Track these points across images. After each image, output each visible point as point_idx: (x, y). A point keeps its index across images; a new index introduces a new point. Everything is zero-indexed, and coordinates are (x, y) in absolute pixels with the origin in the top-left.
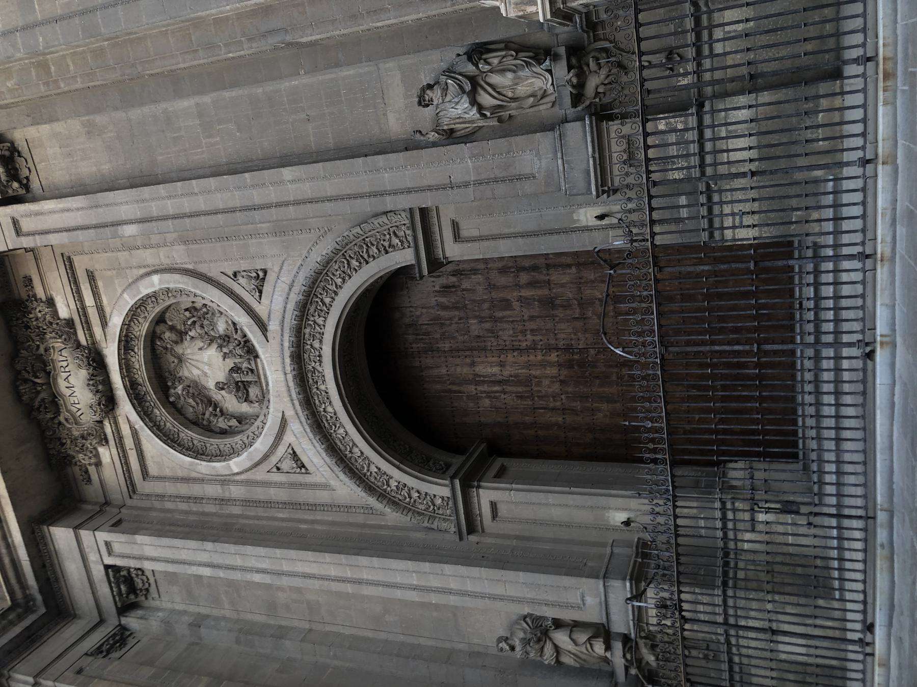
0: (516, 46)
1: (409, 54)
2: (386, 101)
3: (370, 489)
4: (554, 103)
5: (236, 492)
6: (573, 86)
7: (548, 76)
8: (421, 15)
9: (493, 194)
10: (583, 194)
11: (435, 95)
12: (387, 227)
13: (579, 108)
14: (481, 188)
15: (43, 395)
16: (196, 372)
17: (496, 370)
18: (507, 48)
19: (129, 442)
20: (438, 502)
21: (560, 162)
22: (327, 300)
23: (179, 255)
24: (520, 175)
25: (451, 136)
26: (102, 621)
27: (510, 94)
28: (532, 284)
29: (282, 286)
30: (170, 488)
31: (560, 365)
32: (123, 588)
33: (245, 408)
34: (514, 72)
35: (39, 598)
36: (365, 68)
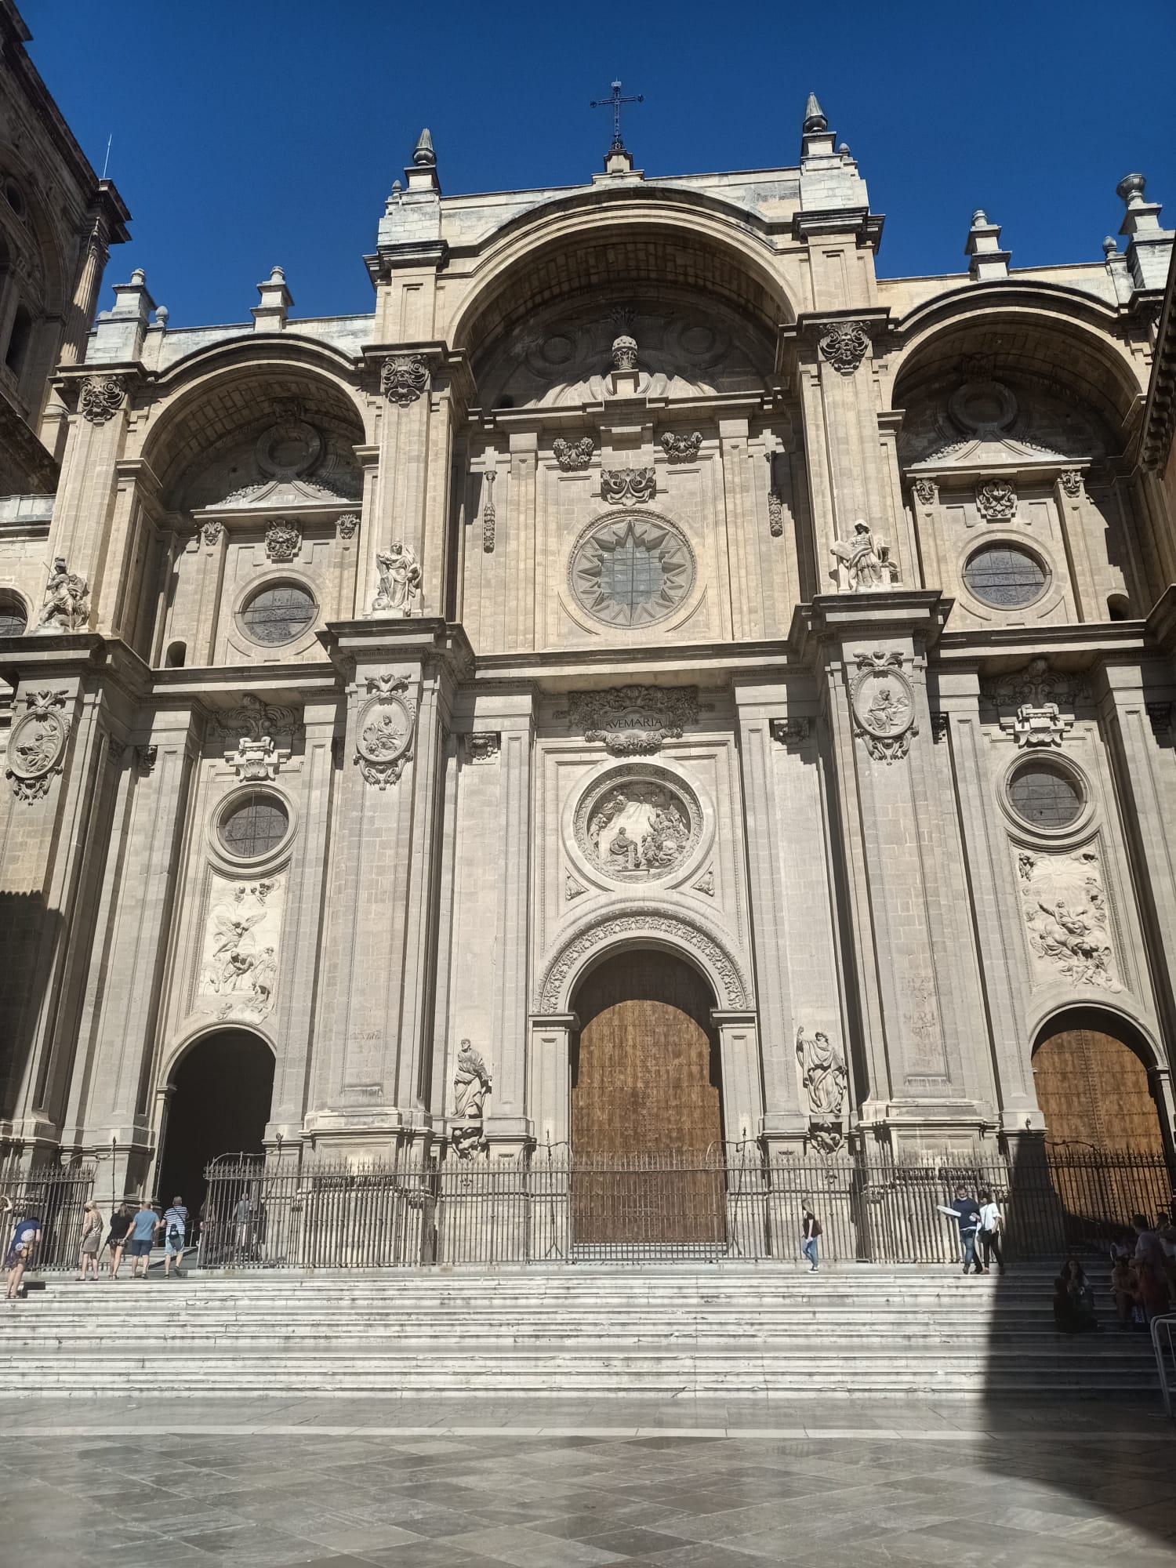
3: (562, 951)
5: (551, 840)
15: (628, 703)
16: (632, 810)
17: (630, 1042)
19: (586, 757)
20: (553, 1000)
22: (694, 940)
23: (726, 833)
25: (800, 1048)
26: (452, 717)
28: (691, 1074)
29: (703, 908)
30: (550, 784)
31: (634, 1088)
32: (481, 741)
33: (604, 846)
35: (479, 675)
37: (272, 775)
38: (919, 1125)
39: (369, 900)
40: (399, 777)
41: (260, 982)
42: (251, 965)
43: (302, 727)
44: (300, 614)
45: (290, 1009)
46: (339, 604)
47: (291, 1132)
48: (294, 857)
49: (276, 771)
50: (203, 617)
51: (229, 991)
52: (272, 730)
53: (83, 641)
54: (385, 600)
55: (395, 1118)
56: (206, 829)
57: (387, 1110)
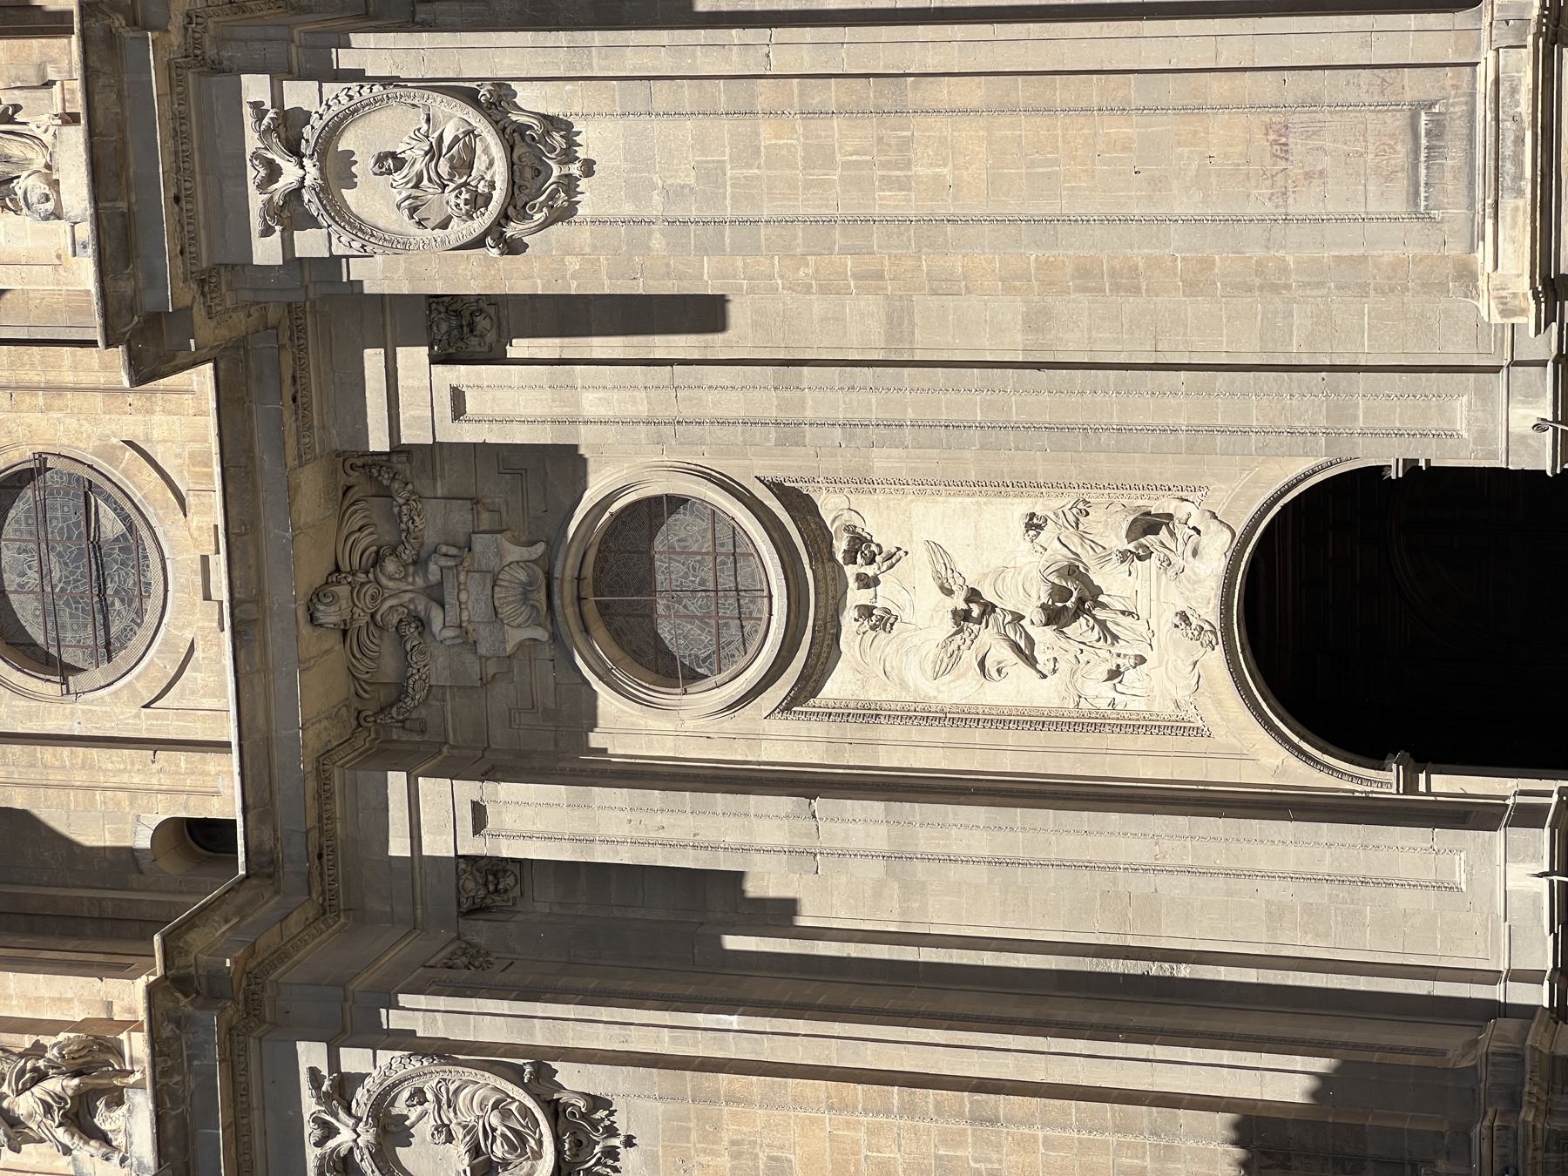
37: (540, 548)
39: (903, 185)
40: (551, 122)
41: (1118, 540)
42: (1072, 571)
43: (399, 449)
44: (64, 512)
45: (1193, 431)
46: (32, 389)
47: (1531, 396)
48: (769, 475)
49: (531, 543)
50: (80, 778)
51: (1141, 626)
52: (408, 555)
53: (167, 1030)
54: (29, 184)
55: (1510, 58)
56: (690, 725)
57: (1483, 85)
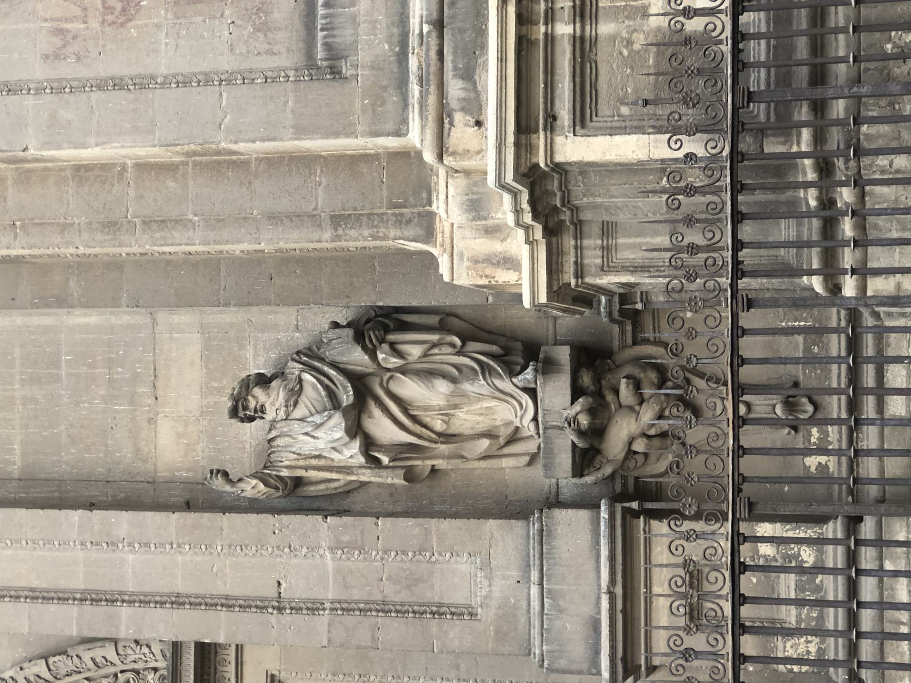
0: (464, 325)
1: (227, 305)
2: (160, 393)
4: (533, 458)
6: (580, 433)
7: (526, 399)
8: (262, 246)
9: (374, 639)
10: (580, 672)
11: (272, 400)
12: (112, 670)
13: (588, 479)
14: (349, 620)
18: (442, 328)
21: (534, 590)
24: (441, 605)
25: (293, 495)
27: (439, 426)
34: (454, 380)
36: (124, 318)
38: (523, 20)
